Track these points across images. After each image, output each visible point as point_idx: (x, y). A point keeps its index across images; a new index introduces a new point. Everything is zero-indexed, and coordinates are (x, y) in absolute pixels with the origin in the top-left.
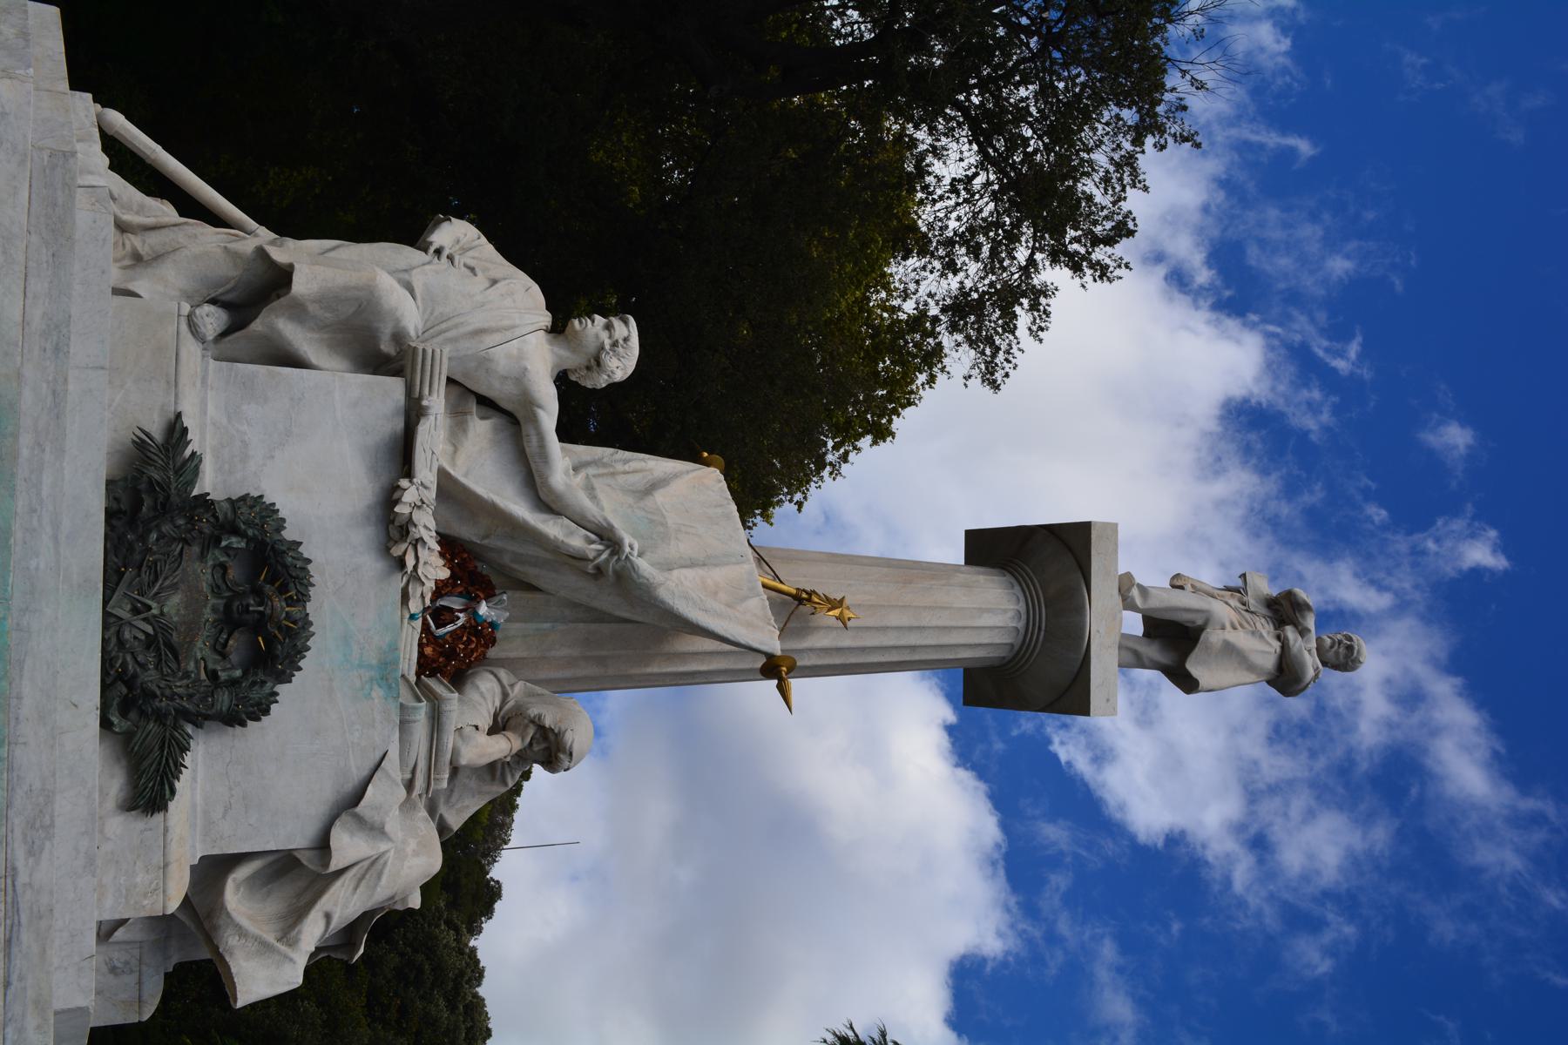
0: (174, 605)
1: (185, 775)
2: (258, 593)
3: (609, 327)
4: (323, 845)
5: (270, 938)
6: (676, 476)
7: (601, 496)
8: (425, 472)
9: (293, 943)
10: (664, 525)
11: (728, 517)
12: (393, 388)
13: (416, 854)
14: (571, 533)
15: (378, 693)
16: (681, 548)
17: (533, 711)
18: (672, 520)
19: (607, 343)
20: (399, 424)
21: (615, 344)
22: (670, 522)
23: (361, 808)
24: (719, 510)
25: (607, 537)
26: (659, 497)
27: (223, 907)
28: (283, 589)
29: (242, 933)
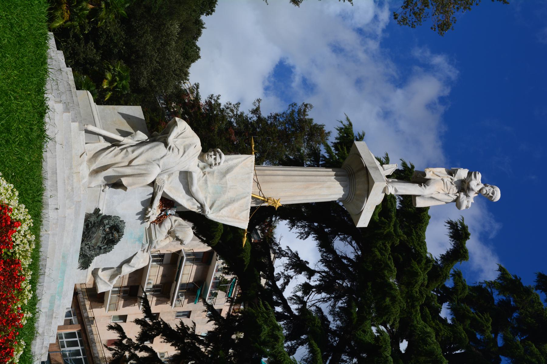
0: (94, 241)
1: (92, 263)
2: (112, 234)
3: (215, 159)
4: (120, 267)
5: (107, 281)
6: (236, 165)
7: (209, 183)
8: (157, 203)
9: (111, 283)
10: (226, 187)
11: (249, 178)
12: (151, 190)
13: (142, 263)
14: (194, 204)
15: (137, 243)
16: (230, 194)
17: (177, 235)
18: (230, 184)
19: (214, 163)
20: (151, 196)
21: (216, 164)
22: (228, 186)
23: (130, 264)
24: (247, 176)
25: (202, 207)
26: (228, 176)
27: (97, 274)
28: (118, 232)
29: (101, 279)
